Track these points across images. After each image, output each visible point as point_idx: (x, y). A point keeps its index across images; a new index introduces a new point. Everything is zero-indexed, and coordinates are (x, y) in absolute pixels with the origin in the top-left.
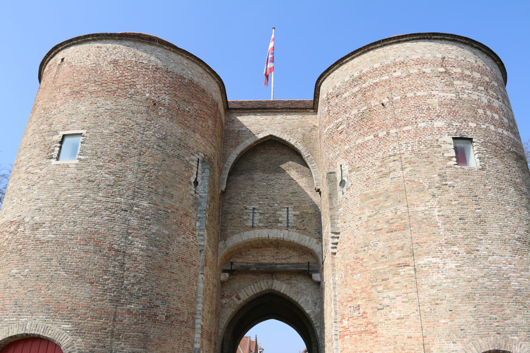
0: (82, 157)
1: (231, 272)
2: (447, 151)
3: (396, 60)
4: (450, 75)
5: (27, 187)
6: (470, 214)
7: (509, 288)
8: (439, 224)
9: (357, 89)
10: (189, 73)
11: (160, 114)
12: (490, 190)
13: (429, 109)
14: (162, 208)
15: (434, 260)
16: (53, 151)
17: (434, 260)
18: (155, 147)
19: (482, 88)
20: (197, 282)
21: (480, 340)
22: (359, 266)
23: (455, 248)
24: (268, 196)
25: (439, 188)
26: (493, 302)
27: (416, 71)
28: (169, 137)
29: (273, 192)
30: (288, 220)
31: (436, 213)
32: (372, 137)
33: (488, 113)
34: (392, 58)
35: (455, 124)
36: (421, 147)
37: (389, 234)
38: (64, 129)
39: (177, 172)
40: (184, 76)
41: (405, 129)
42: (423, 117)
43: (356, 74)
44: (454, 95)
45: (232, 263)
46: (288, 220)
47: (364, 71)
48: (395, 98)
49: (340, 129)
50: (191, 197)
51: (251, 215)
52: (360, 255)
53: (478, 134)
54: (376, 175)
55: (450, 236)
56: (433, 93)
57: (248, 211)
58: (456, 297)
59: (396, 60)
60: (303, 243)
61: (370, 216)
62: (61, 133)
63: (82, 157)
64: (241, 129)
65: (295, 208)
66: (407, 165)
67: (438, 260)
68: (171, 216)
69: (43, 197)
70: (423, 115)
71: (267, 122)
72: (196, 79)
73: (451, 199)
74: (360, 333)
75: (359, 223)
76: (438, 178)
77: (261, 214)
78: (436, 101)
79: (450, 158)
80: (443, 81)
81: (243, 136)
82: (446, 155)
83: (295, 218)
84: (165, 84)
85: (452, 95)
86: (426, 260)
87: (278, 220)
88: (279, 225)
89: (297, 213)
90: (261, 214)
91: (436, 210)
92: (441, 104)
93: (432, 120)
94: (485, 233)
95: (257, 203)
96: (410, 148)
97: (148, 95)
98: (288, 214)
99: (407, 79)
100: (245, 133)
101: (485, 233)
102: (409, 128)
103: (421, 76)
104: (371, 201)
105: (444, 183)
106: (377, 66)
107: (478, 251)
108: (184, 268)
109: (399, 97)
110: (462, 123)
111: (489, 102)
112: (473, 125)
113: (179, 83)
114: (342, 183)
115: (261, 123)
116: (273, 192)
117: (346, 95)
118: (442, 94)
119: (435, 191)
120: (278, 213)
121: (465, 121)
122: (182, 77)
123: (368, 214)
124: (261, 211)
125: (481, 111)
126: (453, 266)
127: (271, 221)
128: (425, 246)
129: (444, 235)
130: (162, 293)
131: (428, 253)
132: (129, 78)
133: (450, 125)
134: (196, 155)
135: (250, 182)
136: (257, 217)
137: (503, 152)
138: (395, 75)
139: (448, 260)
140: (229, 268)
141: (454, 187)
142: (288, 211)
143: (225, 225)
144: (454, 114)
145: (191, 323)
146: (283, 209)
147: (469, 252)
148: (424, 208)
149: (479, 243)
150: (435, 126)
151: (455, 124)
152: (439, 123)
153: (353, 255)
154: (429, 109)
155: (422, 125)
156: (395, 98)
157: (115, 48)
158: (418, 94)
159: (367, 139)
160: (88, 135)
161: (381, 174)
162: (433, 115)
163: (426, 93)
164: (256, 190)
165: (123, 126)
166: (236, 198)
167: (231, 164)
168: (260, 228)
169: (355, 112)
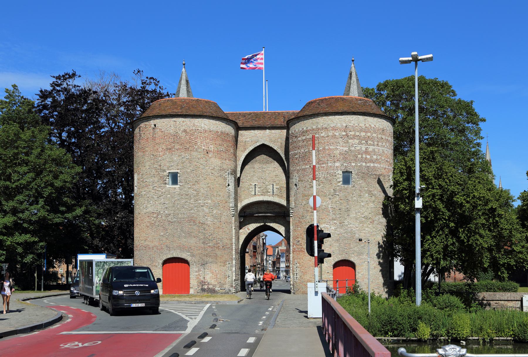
0: (181, 184)
1: (244, 217)
2: (339, 178)
3: (323, 126)
4: (348, 137)
5: (156, 197)
6: (343, 207)
7: (354, 237)
8: (330, 211)
9: (304, 138)
10: (220, 127)
11: (210, 156)
12: (355, 196)
13: (334, 156)
14: (216, 202)
15: (327, 226)
16: (166, 180)
17: (327, 226)
18: (211, 174)
19: (364, 142)
20: (232, 230)
21: (339, 256)
22: (300, 224)
23: (335, 222)
24: (263, 178)
25: (332, 195)
26: (347, 242)
27: (332, 134)
28: (216, 168)
29: (265, 175)
30: (273, 191)
31: (330, 206)
32: (308, 167)
33: (364, 156)
34: (322, 124)
35: (345, 164)
36: (328, 176)
37: (311, 213)
38: (168, 170)
39: (221, 184)
40: (218, 131)
41: (323, 165)
42: (331, 160)
43: (305, 129)
44: (347, 148)
45: (245, 212)
46: (273, 191)
47: (309, 128)
48: (320, 148)
49: (296, 156)
50: (227, 193)
51: (254, 188)
52: (301, 220)
53: (355, 169)
54: (309, 186)
55: (334, 216)
56: (338, 147)
57: (252, 186)
58: (333, 240)
59: (323, 126)
60: (281, 203)
61: (305, 204)
62: (168, 171)
63: (181, 184)
64: (246, 140)
65: (277, 184)
66: (321, 184)
67: (328, 226)
68: (220, 204)
69: (167, 203)
70: (331, 159)
71: (261, 135)
72: (223, 130)
73: (337, 201)
74: (299, 251)
75: (301, 206)
76: (332, 191)
77: (259, 188)
78: (338, 152)
79: (339, 182)
80: (343, 140)
81: (248, 144)
82: (338, 180)
83: (277, 190)
84: (210, 139)
85: (346, 149)
86: (324, 225)
87: (268, 191)
88: (269, 193)
89: (278, 187)
90: (259, 188)
91: (330, 205)
92: (340, 154)
93: (334, 162)
94: (348, 215)
95: (257, 181)
96: (323, 176)
97: (203, 147)
98: (273, 188)
99: (327, 138)
100: (248, 142)
101: (348, 215)
102: (324, 165)
103: (334, 137)
104: (306, 197)
105: (335, 193)
106: (314, 127)
107: (344, 223)
108: (227, 226)
109: (322, 148)
110: (348, 164)
111: (366, 149)
112: (353, 164)
113: (216, 136)
114: (296, 185)
115: (257, 136)
116: (265, 175)
117: (300, 139)
118: (342, 148)
119: (331, 196)
120: (268, 187)
121: (350, 163)
122: (217, 132)
123: (305, 203)
124: (259, 186)
125: (359, 156)
126: (333, 228)
127: (264, 191)
128: (324, 220)
129: (332, 216)
130: (220, 238)
131: (325, 223)
132: (194, 139)
133: (342, 165)
134: (228, 172)
135: (252, 169)
136: (257, 189)
137: (367, 176)
138: (322, 135)
139: (332, 226)
140: (243, 215)
141: (339, 195)
142: (273, 186)
143: (240, 194)
144: (345, 159)
145: (231, 248)
146: (271, 185)
147: (340, 223)
148: (325, 204)
149: (345, 220)
150: (335, 166)
151: (345, 164)
152: (337, 164)
153: (298, 219)
154: (334, 156)
155: (330, 164)
156: (320, 148)
157: (183, 122)
158: (331, 147)
159: (306, 167)
160: (181, 173)
161: (310, 186)
162: (336, 160)
163: (334, 148)
164: (256, 174)
165: (196, 167)
166: (245, 179)
167: (242, 162)
168: (259, 195)
169: (303, 150)
